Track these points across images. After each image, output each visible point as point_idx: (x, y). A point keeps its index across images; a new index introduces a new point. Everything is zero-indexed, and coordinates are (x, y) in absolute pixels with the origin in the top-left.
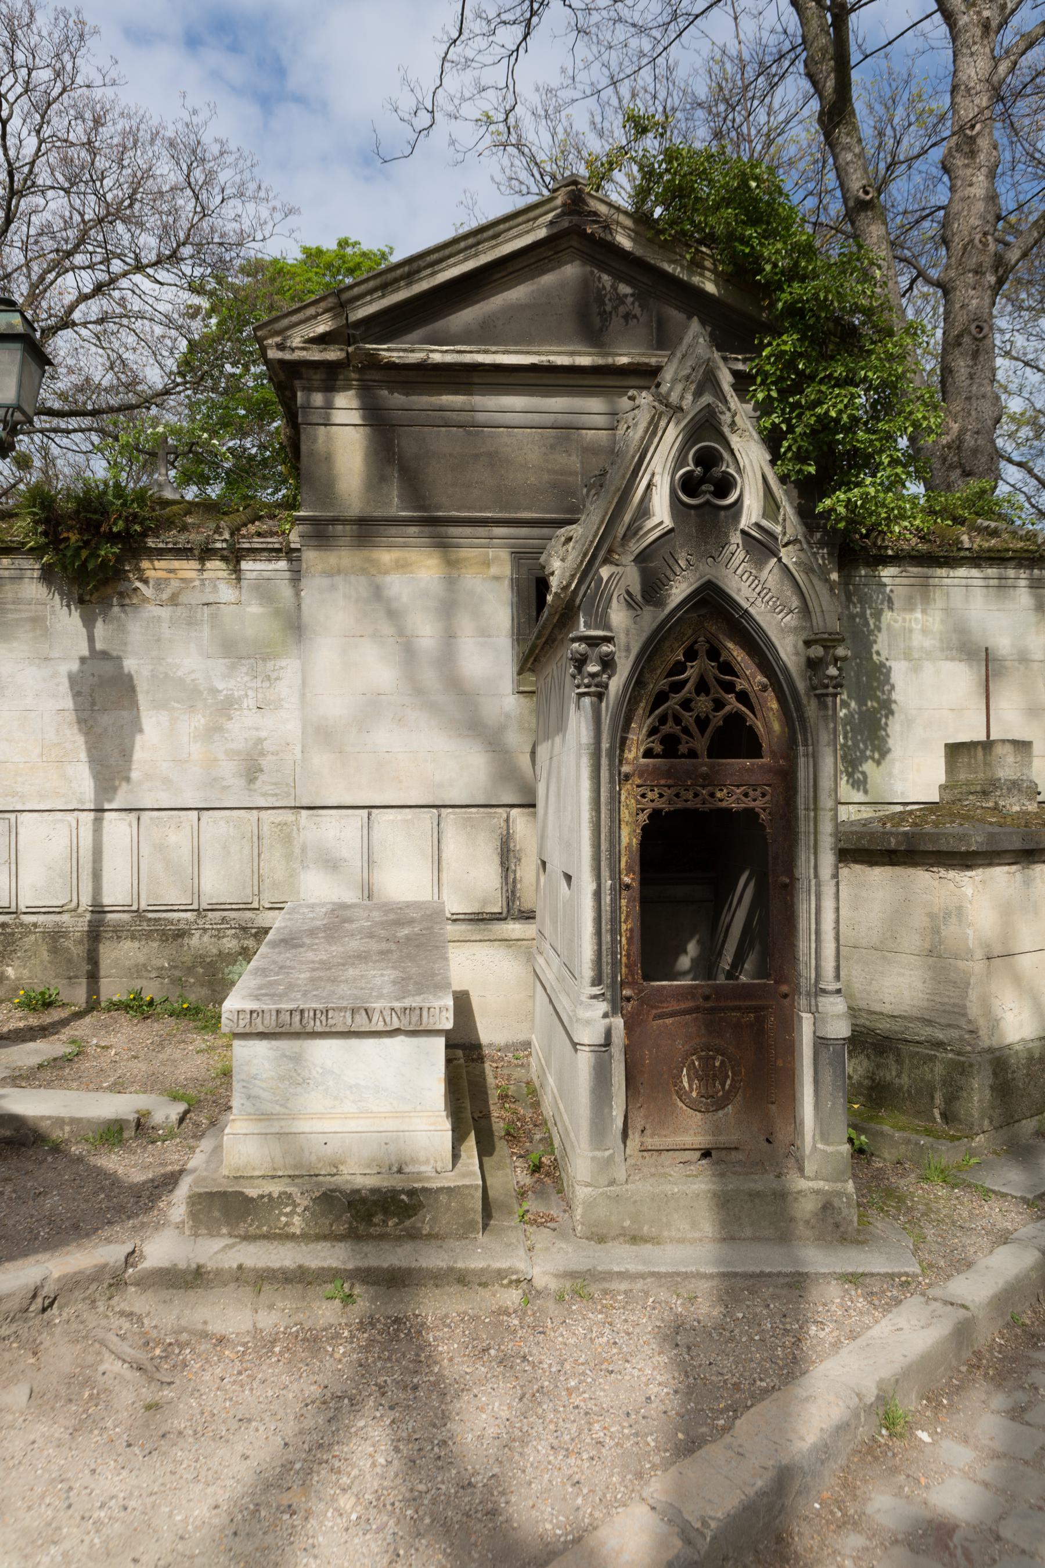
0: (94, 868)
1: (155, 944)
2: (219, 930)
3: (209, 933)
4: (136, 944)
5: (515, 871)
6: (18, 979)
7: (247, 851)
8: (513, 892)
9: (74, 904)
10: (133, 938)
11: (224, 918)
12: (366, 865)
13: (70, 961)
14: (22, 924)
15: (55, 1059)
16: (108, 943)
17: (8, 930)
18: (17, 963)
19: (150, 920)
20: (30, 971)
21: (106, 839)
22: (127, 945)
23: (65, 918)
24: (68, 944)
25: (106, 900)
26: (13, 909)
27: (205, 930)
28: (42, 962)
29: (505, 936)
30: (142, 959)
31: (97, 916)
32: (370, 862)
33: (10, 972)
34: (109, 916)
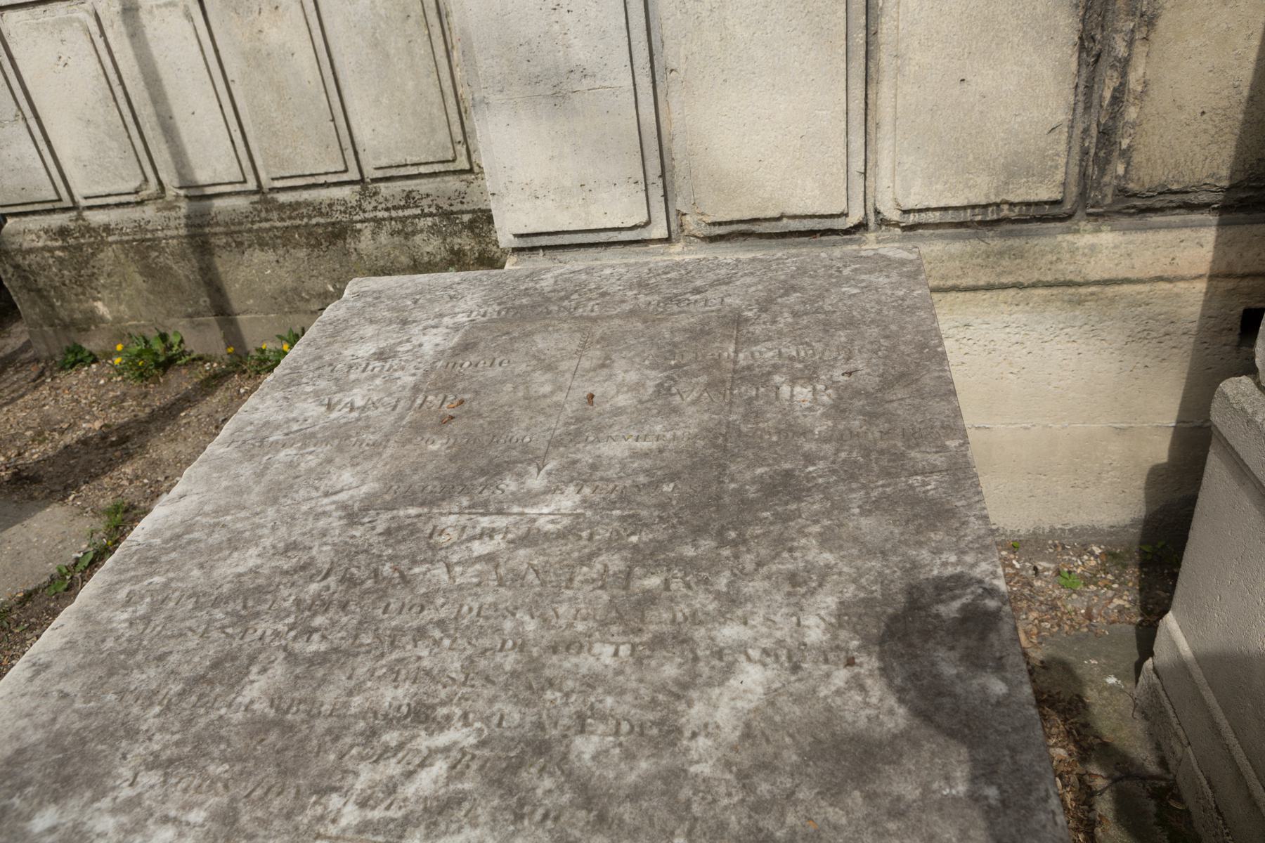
0: (158, 115)
1: (302, 253)
2: (403, 220)
3: (387, 227)
4: (271, 255)
5: (1124, 65)
6: (118, 320)
7: (421, 49)
8: (1107, 135)
9: (153, 186)
10: (262, 245)
11: (409, 195)
12: (644, 83)
13: (178, 288)
14: (89, 229)
15: (29, 596)
16: (225, 255)
17: (71, 241)
18: (105, 294)
19: (282, 207)
20: (130, 307)
21: (156, 50)
22: (258, 256)
23: (149, 212)
24: (166, 260)
25: (202, 176)
26: (67, 202)
27: (378, 222)
28: (139, 292)
29: (1067, 270)
30: (289, 282)
31: (197, 205)
32: (655, 68)
33: (101, 308)
34: (218, 203)
